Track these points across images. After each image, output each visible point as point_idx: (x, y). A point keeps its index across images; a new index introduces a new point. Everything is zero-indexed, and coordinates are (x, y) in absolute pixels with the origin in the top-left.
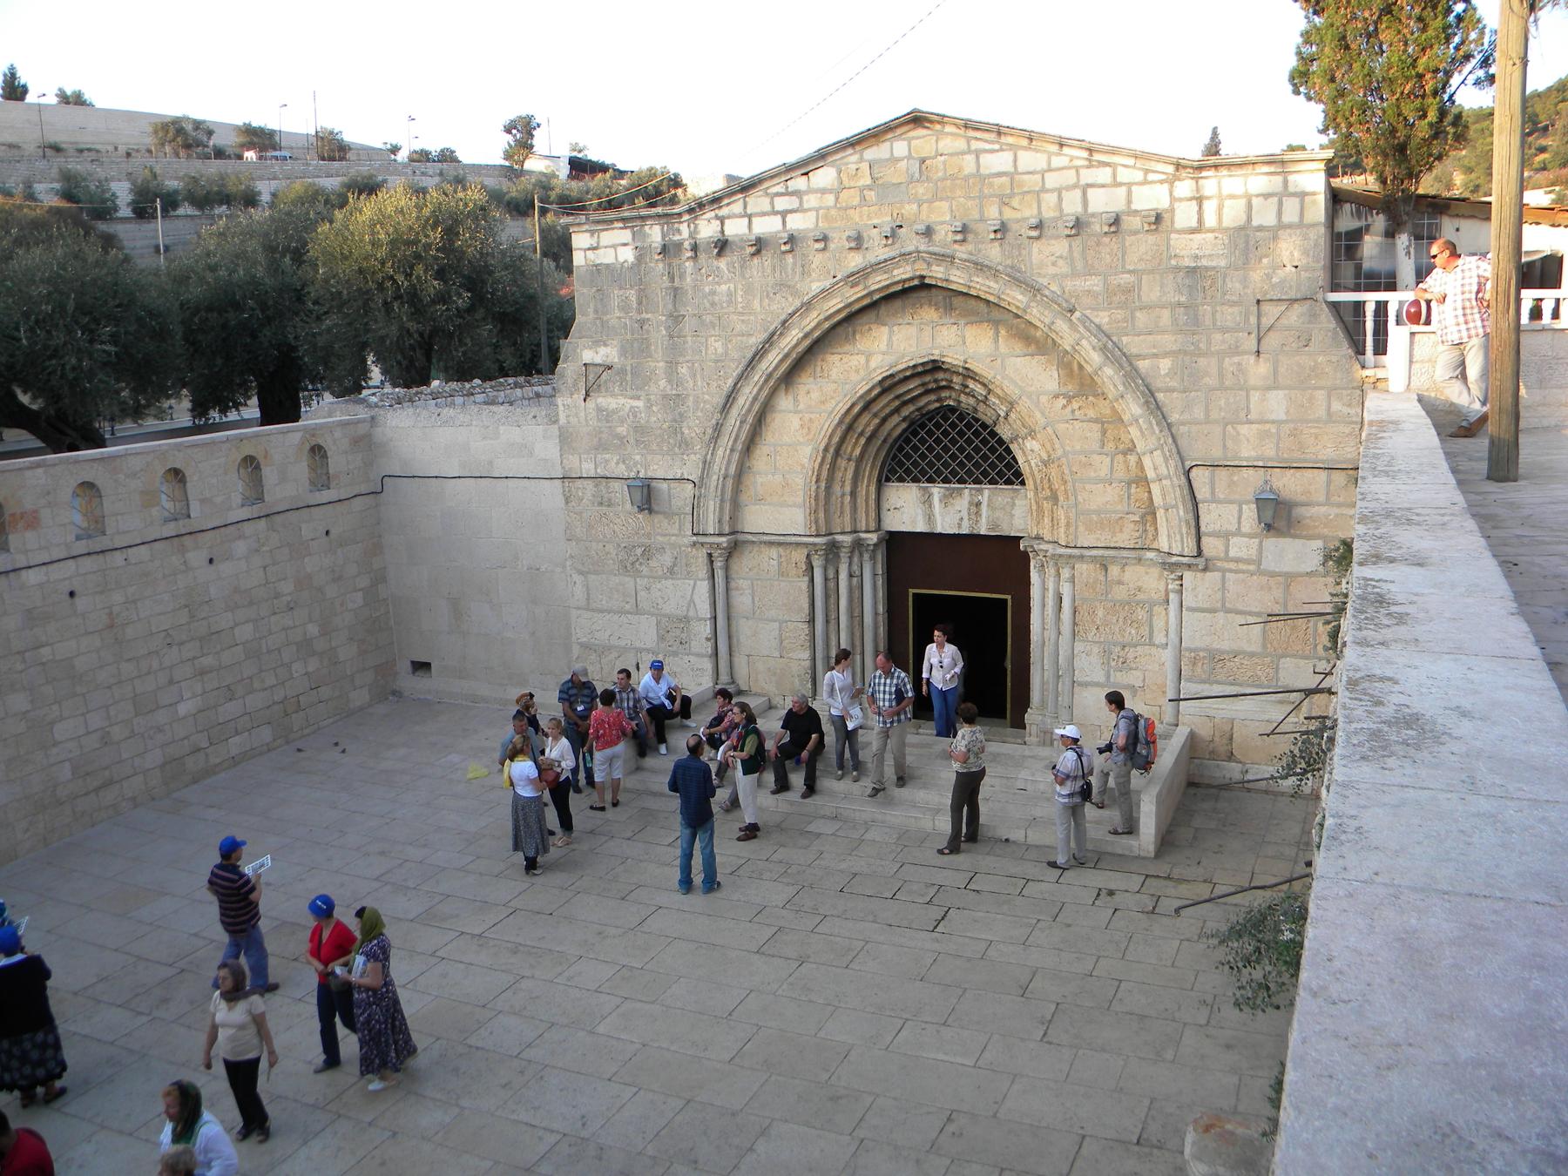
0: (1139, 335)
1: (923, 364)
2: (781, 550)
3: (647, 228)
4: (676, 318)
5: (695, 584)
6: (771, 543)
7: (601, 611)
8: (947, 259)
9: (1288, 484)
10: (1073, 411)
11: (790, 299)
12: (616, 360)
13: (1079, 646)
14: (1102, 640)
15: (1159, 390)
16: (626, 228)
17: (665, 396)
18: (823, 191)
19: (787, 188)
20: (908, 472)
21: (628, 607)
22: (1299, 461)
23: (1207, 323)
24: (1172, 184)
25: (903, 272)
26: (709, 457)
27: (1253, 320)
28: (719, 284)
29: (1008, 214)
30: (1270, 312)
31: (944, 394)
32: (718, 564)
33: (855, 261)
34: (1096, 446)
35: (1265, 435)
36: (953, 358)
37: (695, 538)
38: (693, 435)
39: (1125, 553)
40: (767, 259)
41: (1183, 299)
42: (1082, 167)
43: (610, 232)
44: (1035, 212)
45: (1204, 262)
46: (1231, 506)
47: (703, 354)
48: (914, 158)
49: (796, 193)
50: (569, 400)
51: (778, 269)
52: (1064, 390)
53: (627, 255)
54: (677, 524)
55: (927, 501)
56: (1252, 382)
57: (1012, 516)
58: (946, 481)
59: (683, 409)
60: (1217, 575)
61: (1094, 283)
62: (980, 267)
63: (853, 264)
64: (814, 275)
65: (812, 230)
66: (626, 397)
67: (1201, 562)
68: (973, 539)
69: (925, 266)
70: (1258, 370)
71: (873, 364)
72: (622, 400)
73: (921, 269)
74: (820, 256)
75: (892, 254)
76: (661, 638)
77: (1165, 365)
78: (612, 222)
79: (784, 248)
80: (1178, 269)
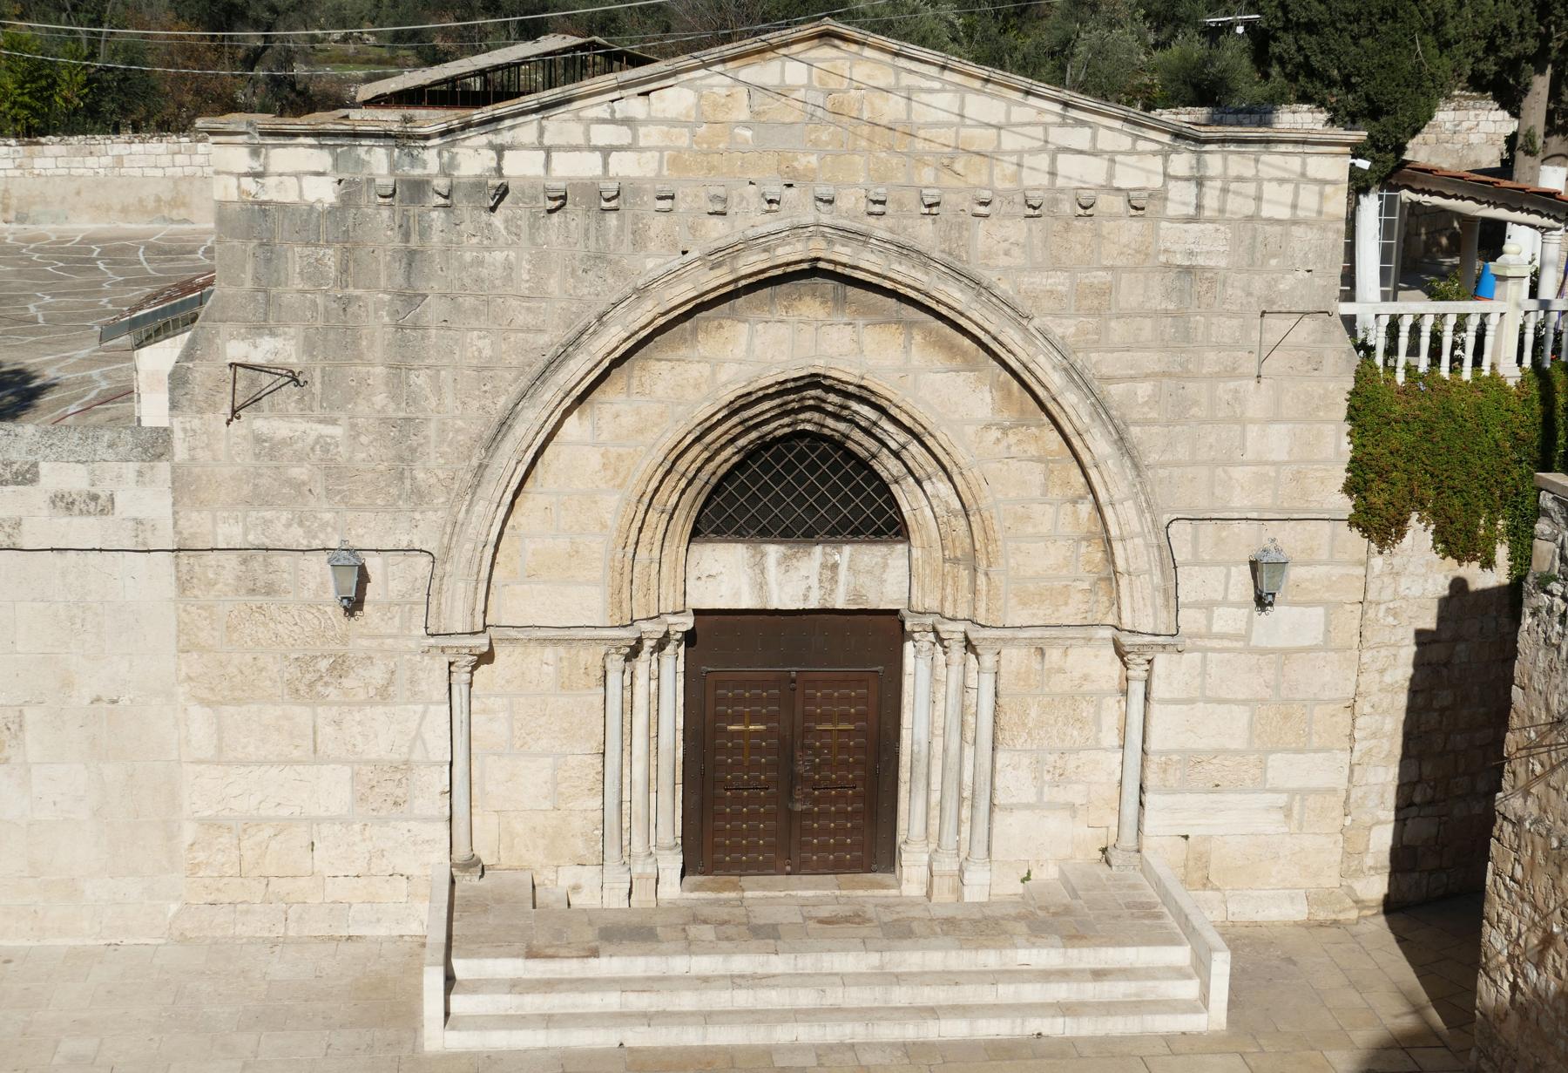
0: (1112, 352)
1: (794, 380)
2: (562, 650)
3: (361, 152)
4: (410, 298)
5: (425, 713)
6: (543, 641)
7: (244, 763)
8: (862, 237)
10: (1009, 447)
11: (610, 281)
12: (293, 360)
13: (1001, 758)
14: (1035, 747)
15: (1136, 423)
16: (321, 146)
17: (384, 421)
18: (673, 123)
19: (613, 112)
21: (296, 754)
22: (1298, 511)
23: (1199, 338)
24: (1166, 156)
25: (792, 252)
26: (461, 516)
27: (1255, 336)
28: (488, 249)
32: (461, 676)
33: (717, 232)
34: (1037, 493)
36: (846, 370)
37: (432, 641)
38: (433, 481)
39: (1070, 633)
40: (575, 218)
41: (1172, 307)
42: (1053, 124)
43: (290, 150)
44: (985, 179)
45: (1201, 261)
46: (1217, 569)
47: (457, 357)
48: (815, 89)
49: (627, 122)
50: (196, 423)
51: (592, 232)
52: (998, 418)
53: (323, 192)
54: (397, 621)
56: (1250, 414)
57: (883, 582)
59: (414, 441)
60: (1197, 656)
62: (905, 251)
63: (714, 235)
64: (652, 246)
65: (651, 179)
66: (310, 419)
69: (823, 245)
70: (1257, 400)
71: (723, 377)
72: (301, 426)
73: (817, 248)
74: (663, 218)
75: (771, 228)
76: (362, 799)
77: (1144, 389)
78: (295, 135)
79: (605, 205)
80: (1167, 266)
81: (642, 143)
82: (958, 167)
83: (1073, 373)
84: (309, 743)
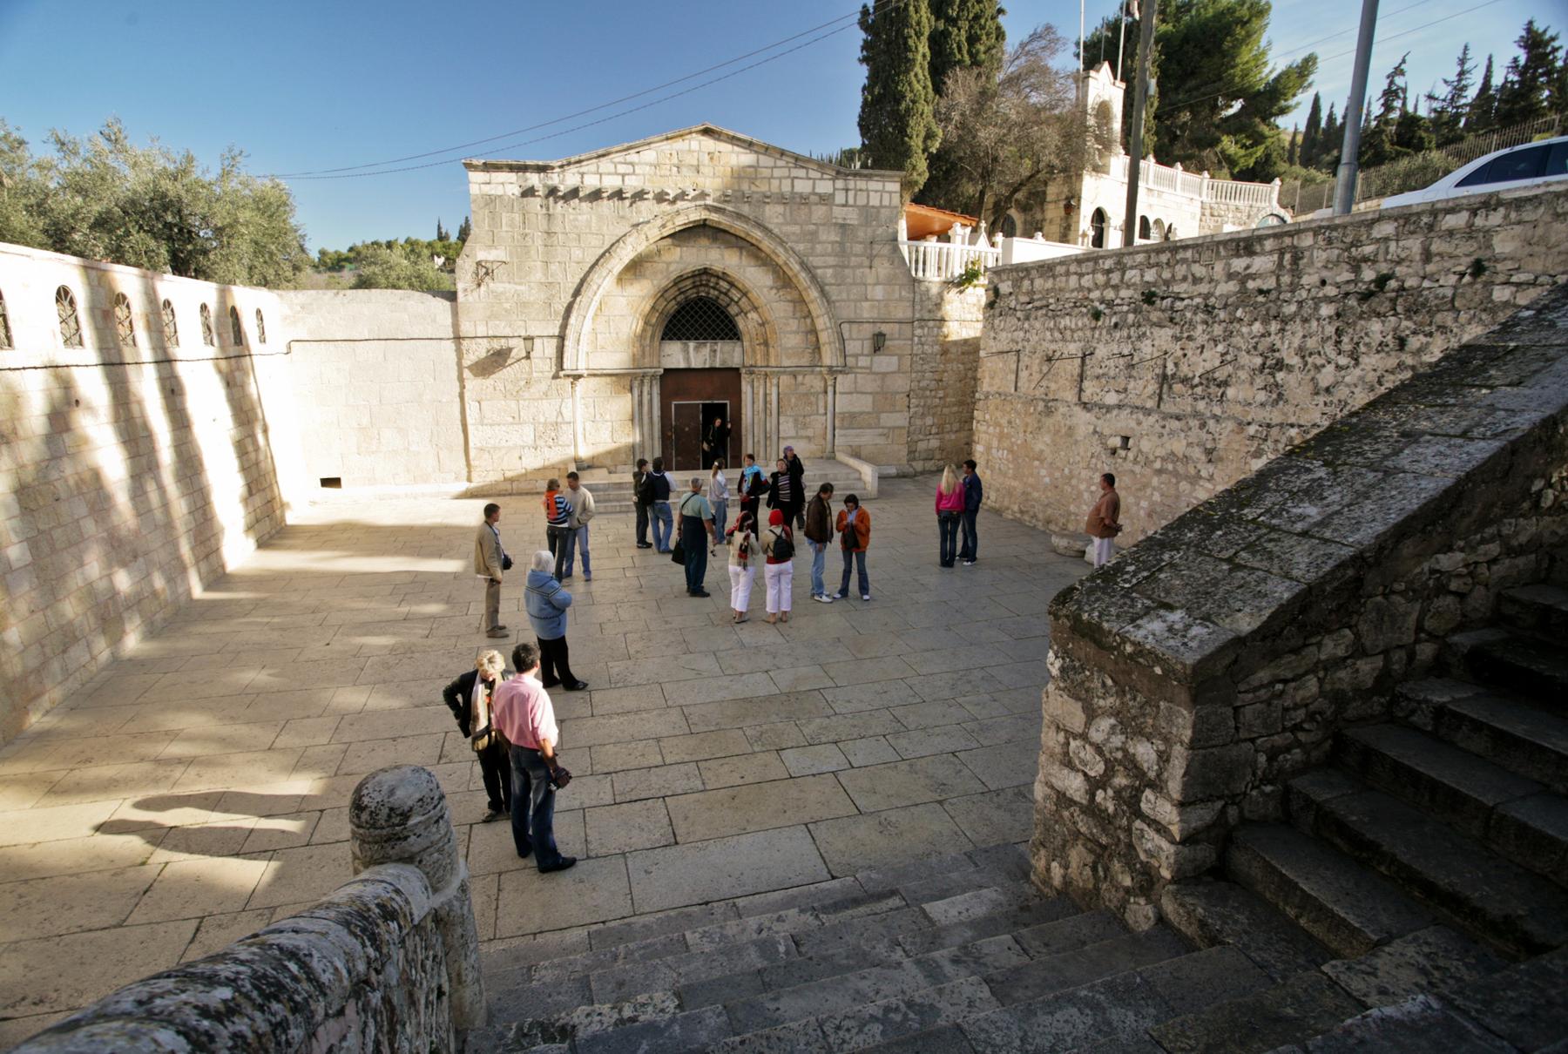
9: (885, 328)
13: (782, 419)
20: (675, 334)
29: (754, 188)
30: (877, 247)
31: (702, 289)
35: (873, 307)
36: (718, 267)
49: (632, 164)
55: (686, 351)
58: (696, 339)
61: (796, 229)
62: (739, 216)
67: (847, 370)
68: (712, 370)
71: (671, 269)
72: (507, 285)
77: (830, 272)
81: (637, 171)
82: (757, 183)
83: (805, 266)
84: (516, 416)
